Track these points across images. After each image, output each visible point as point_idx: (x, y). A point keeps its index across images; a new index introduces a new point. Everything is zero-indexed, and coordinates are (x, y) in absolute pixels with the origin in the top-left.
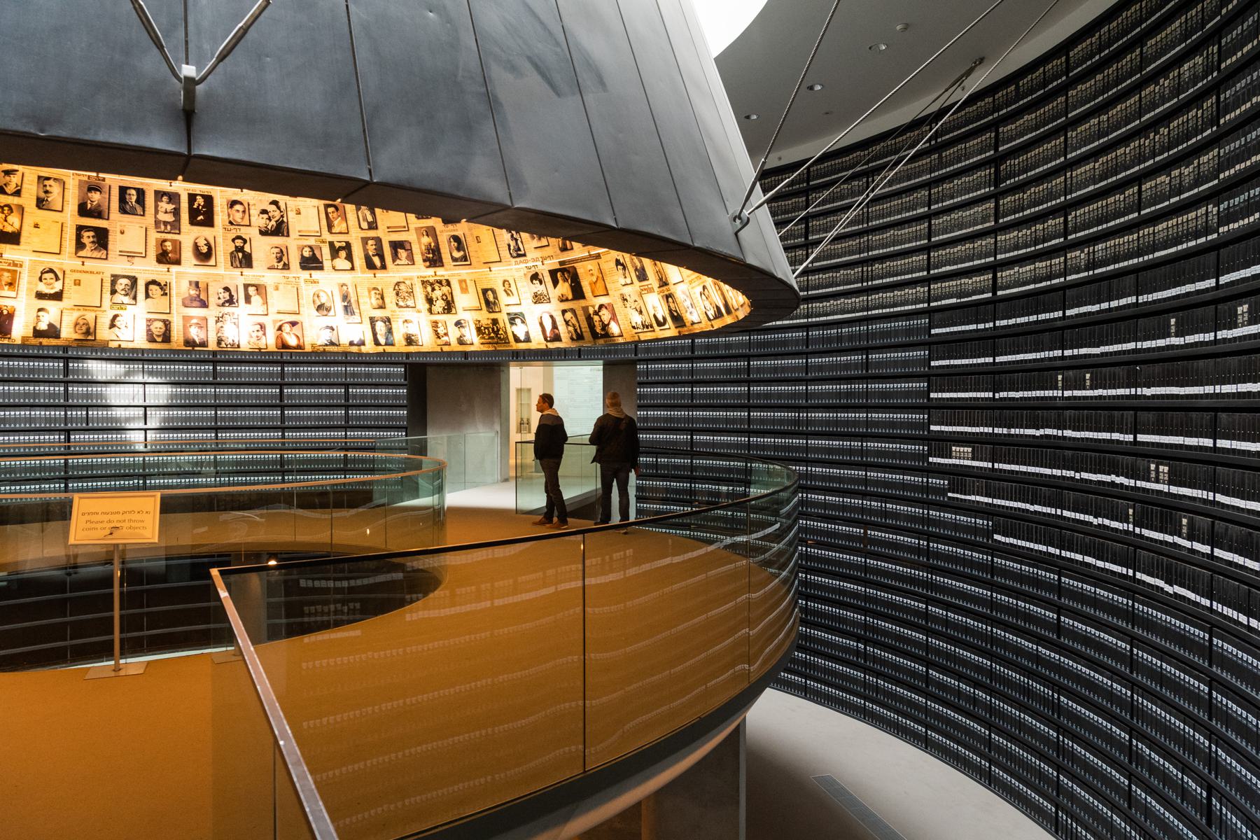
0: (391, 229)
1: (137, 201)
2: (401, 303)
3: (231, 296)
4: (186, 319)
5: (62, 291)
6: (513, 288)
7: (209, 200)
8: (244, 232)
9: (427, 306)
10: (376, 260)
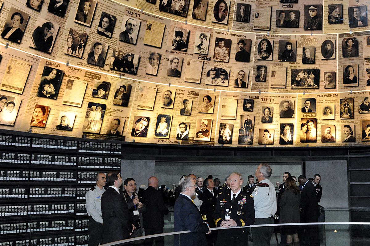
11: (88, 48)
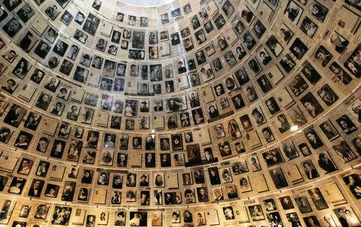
0: (53, 179)
2: (38, 216)
6: (106, 217)
9: (53, 219)
10: (36, 192)
11: (352, 148)
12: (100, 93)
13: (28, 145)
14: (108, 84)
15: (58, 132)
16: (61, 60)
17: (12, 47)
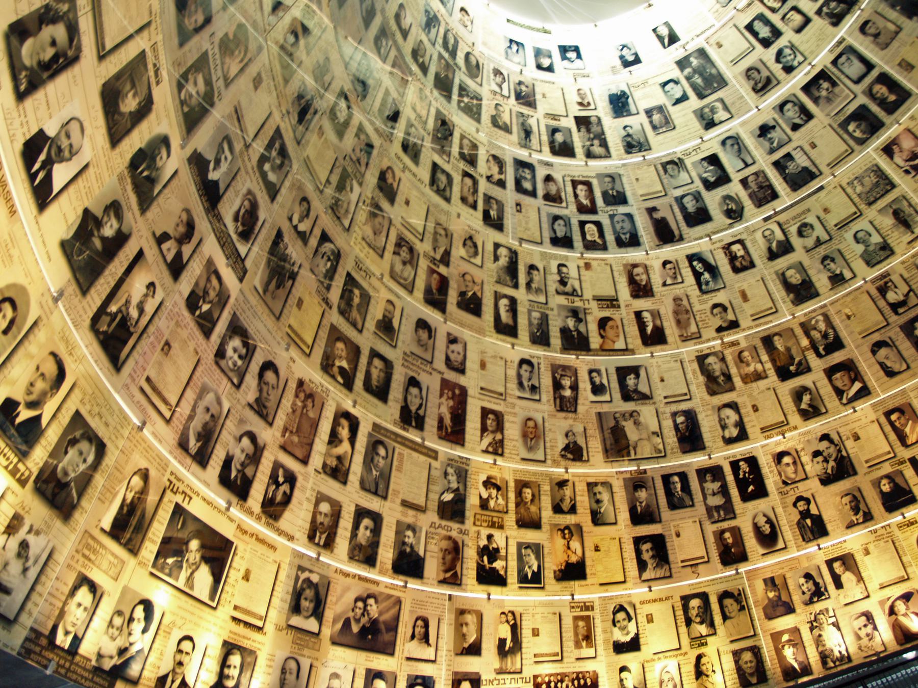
1: (682, 489)
3: (816, 584)
4: (776, 637)
5: (637, 635)
7: (752, 461)
8: (803, 489)
12: (871, 152)
13: (863, 381)
14: (866, 122)
15: (887, 310)
16: (735, 188)
17: (658, 258)
